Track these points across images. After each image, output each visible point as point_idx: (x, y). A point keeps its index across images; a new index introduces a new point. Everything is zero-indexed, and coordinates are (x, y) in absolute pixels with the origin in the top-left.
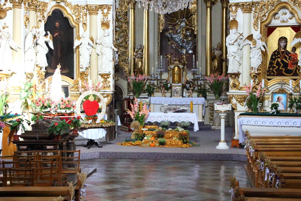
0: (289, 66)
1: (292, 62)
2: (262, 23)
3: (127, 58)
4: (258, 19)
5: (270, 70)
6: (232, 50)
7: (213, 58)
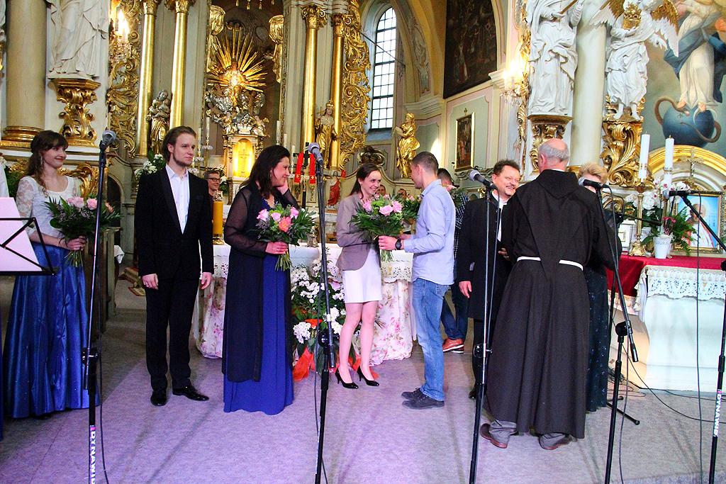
7: (317, 131)
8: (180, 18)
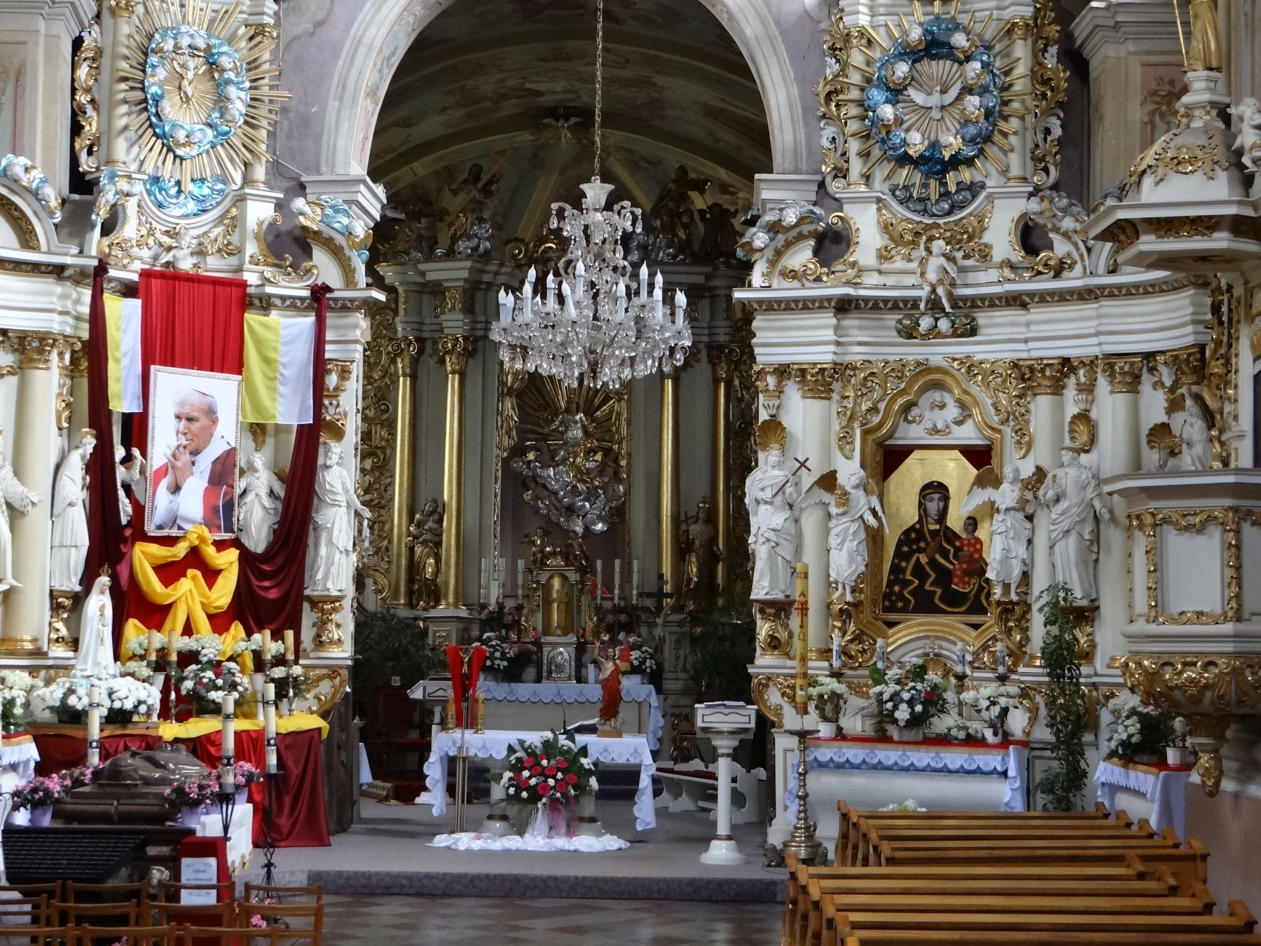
0: (956, 580)
1: (965, 566)
2: (865, 433)
3: (385, 543)
4: (852, 418)
5: (892, 593)
6: (765, 521)
7: (682, 549)
8: (453, 383)
